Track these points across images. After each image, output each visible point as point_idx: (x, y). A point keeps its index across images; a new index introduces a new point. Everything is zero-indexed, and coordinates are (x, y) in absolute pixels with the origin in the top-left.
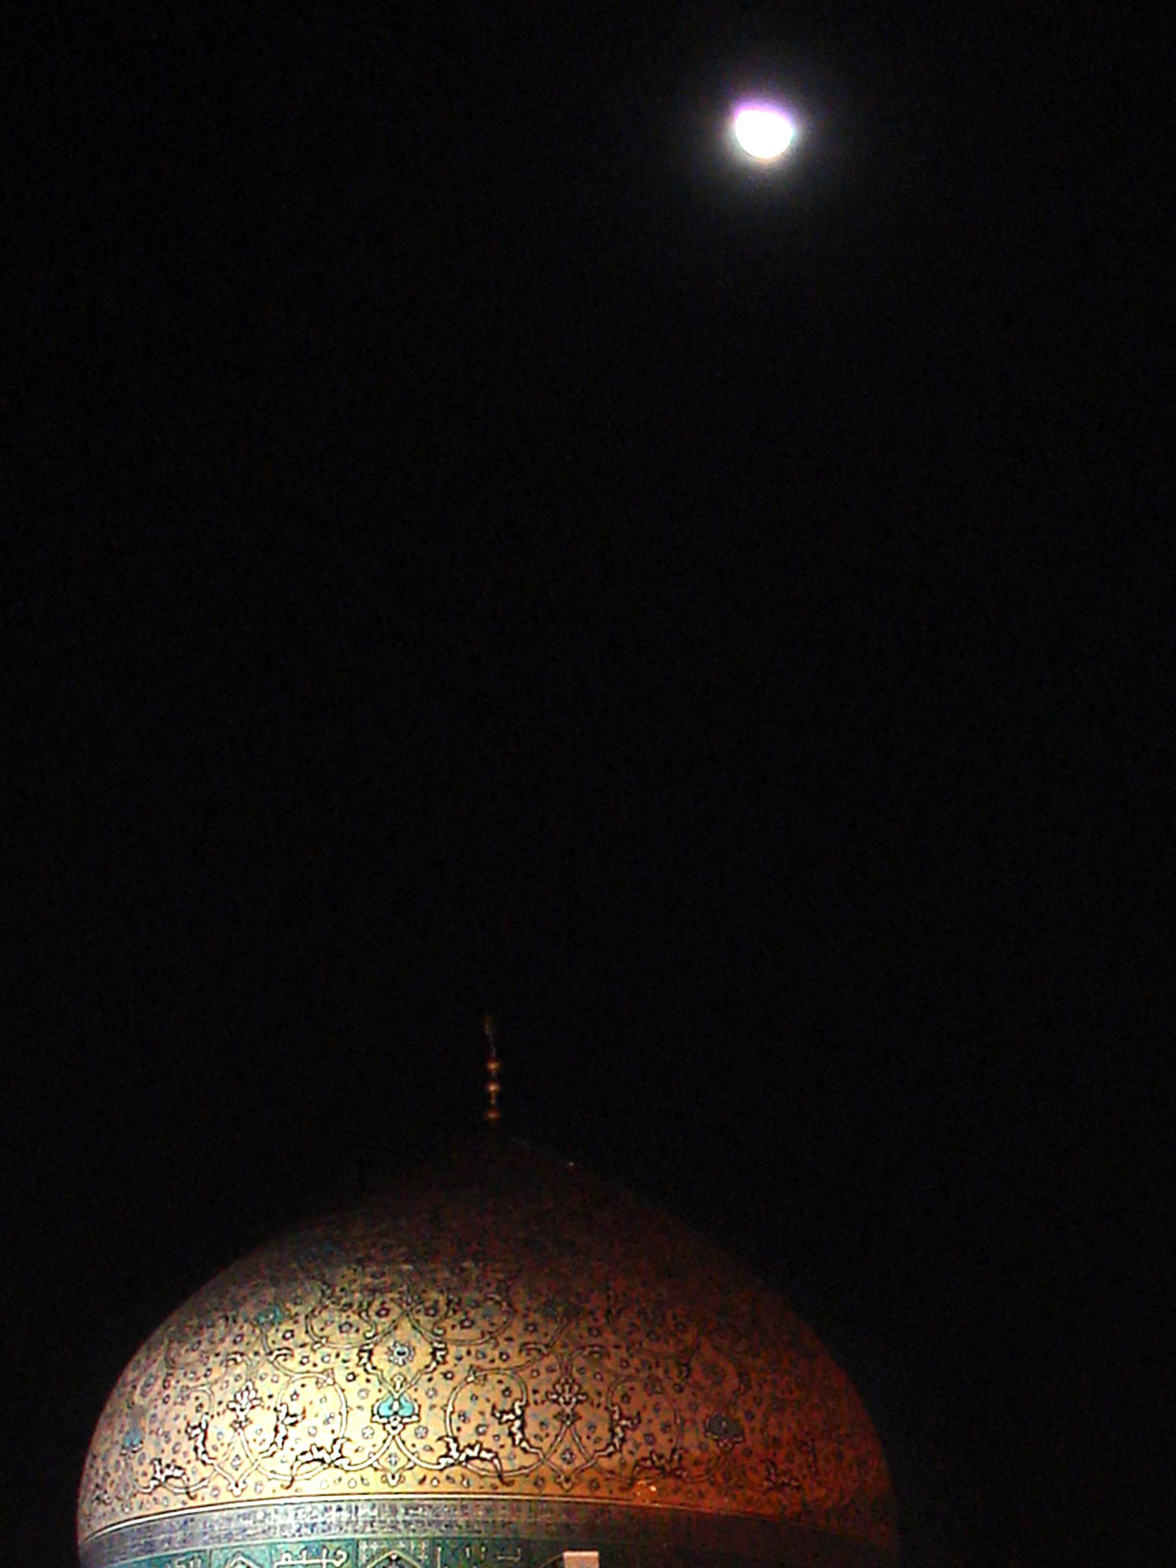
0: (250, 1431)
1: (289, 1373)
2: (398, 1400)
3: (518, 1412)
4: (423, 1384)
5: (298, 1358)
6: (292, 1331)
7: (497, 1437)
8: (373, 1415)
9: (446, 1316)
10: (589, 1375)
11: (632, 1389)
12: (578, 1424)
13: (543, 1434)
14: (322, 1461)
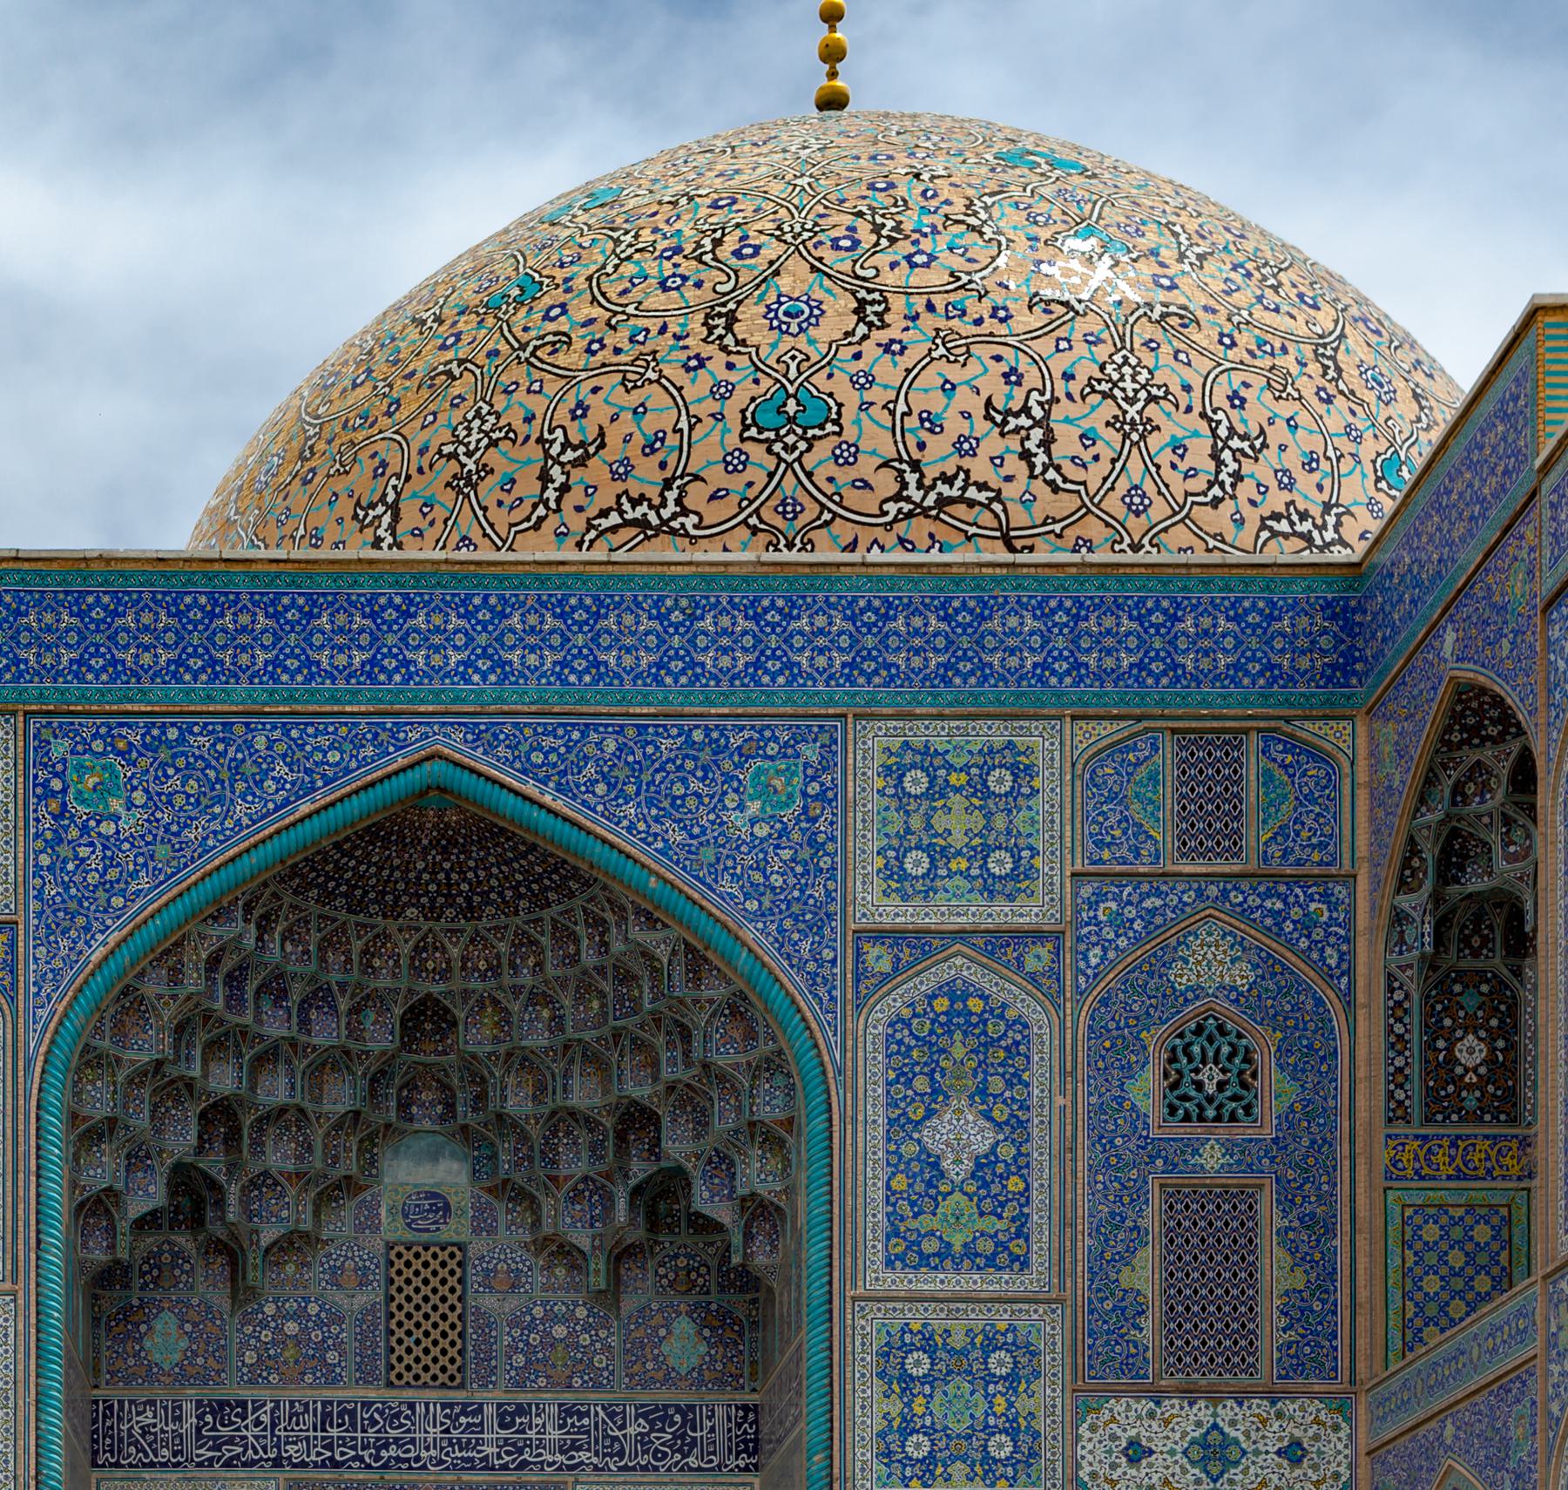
6: (563, 306)
7: (997, 461)
8: (746, 428)
12: (1154, 441)
13: (1087, 456)
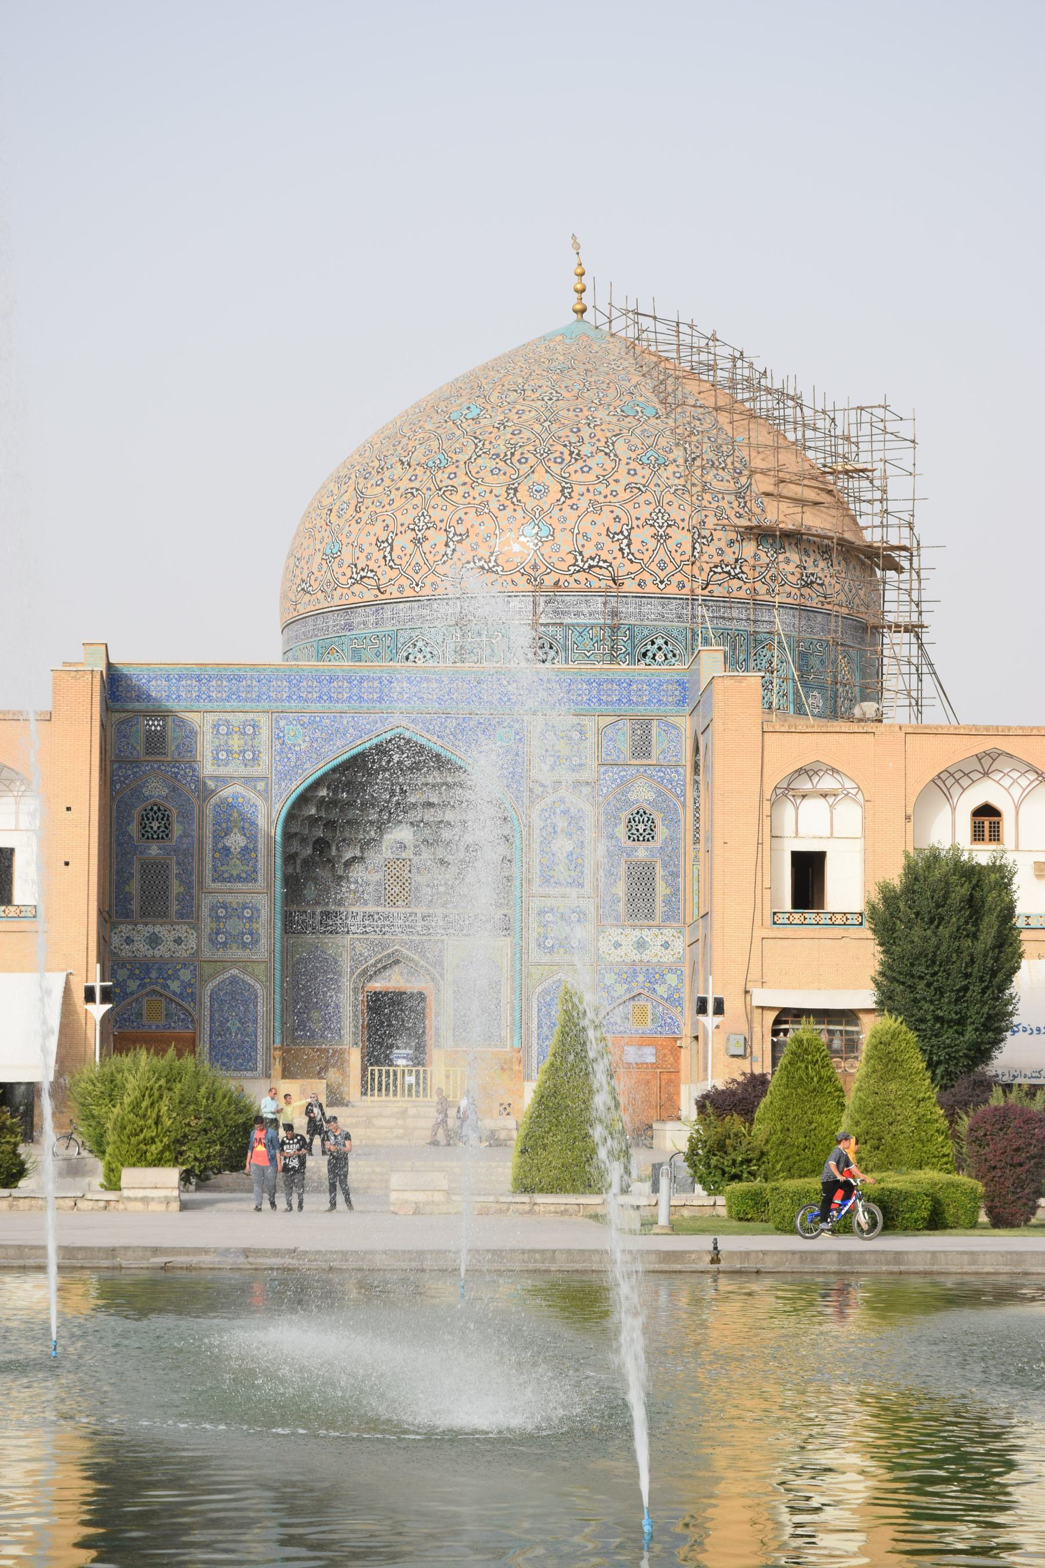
0: (426, 546)
1: (455, 505)
3: (626, 533)
4: (556, 513)
7: (611, 552)
9: (569, 465)
10: (676, 505)
11: (706, 516)
13: (644, 549)
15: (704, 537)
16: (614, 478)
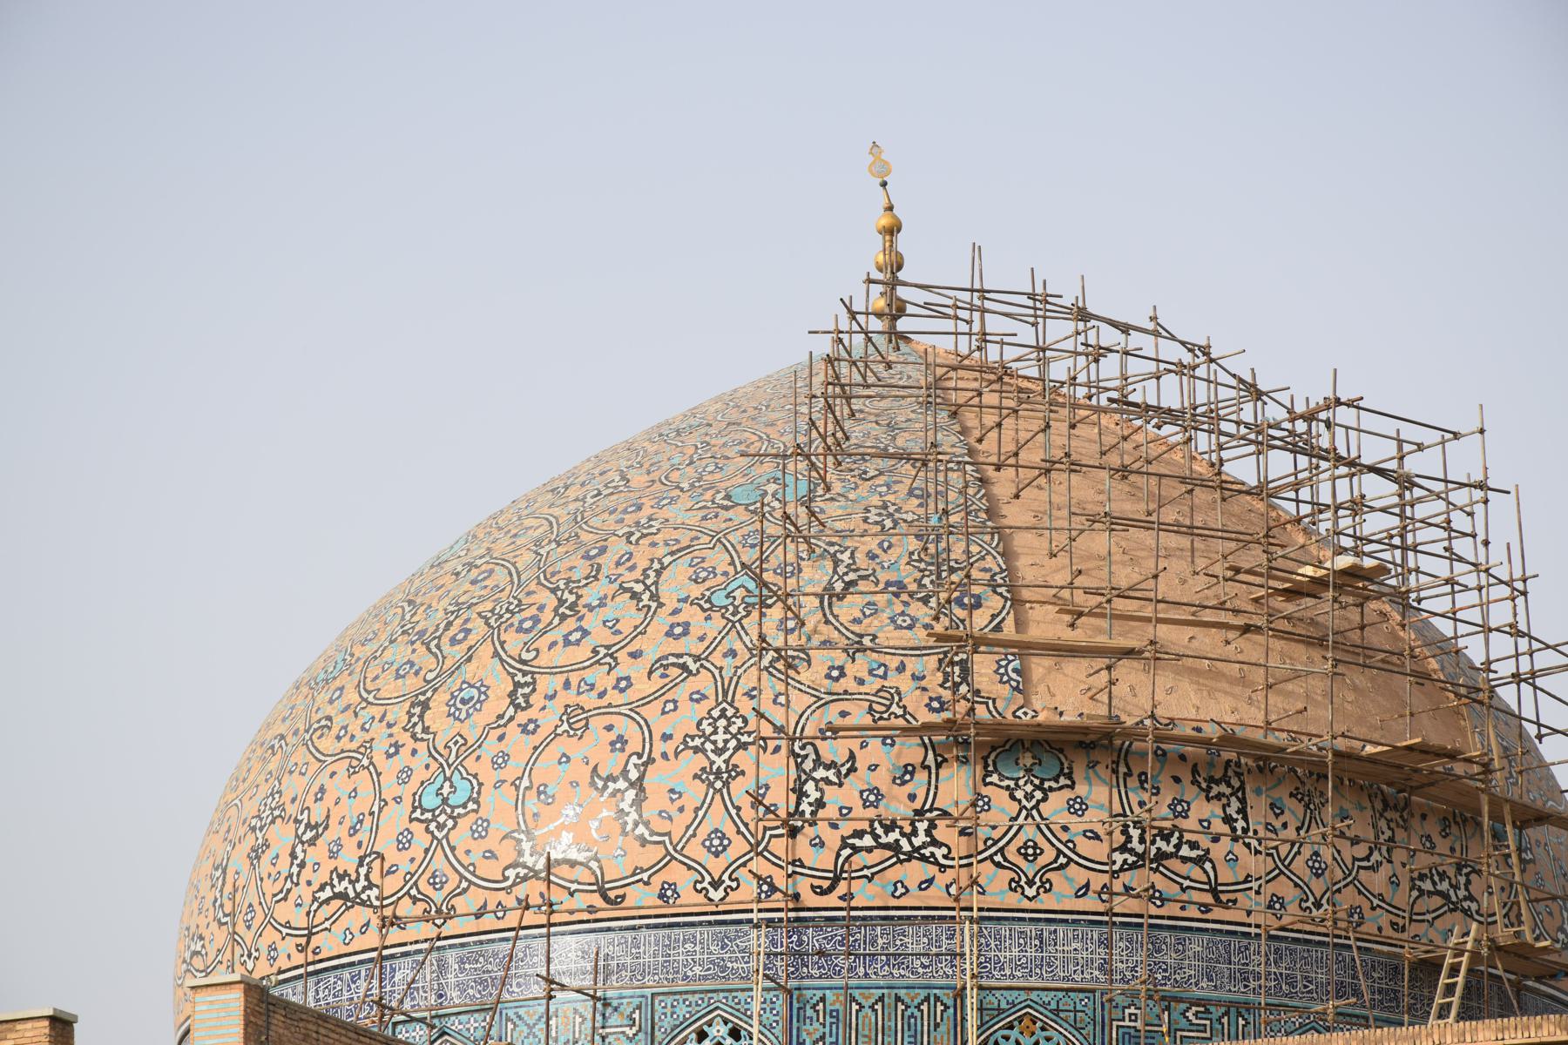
2: (450, 779)
3: (634, 775)
4: (491, 747)
5: (335, 731)
14: (343, 896)
15: (831, 765)
16: (630, 649)
